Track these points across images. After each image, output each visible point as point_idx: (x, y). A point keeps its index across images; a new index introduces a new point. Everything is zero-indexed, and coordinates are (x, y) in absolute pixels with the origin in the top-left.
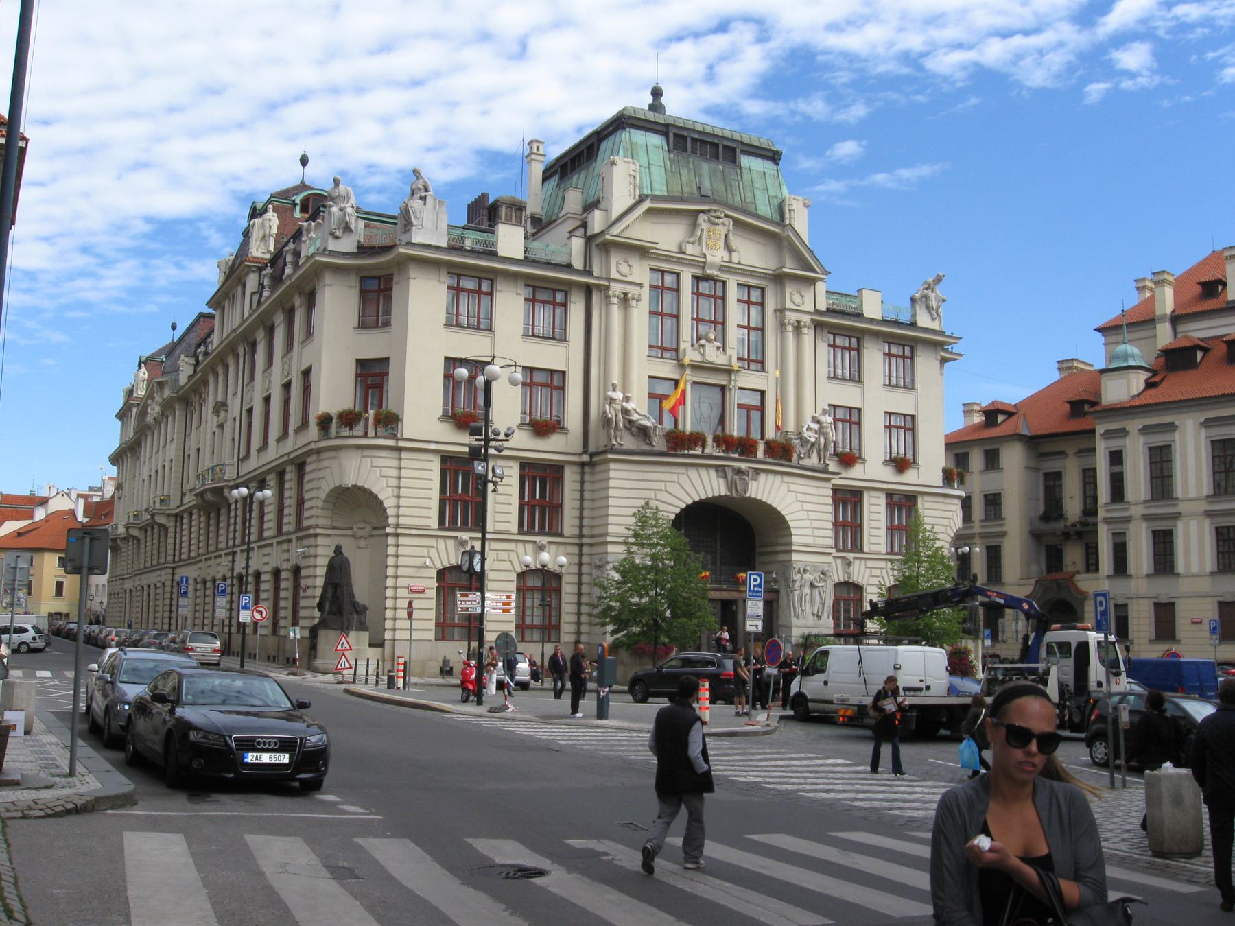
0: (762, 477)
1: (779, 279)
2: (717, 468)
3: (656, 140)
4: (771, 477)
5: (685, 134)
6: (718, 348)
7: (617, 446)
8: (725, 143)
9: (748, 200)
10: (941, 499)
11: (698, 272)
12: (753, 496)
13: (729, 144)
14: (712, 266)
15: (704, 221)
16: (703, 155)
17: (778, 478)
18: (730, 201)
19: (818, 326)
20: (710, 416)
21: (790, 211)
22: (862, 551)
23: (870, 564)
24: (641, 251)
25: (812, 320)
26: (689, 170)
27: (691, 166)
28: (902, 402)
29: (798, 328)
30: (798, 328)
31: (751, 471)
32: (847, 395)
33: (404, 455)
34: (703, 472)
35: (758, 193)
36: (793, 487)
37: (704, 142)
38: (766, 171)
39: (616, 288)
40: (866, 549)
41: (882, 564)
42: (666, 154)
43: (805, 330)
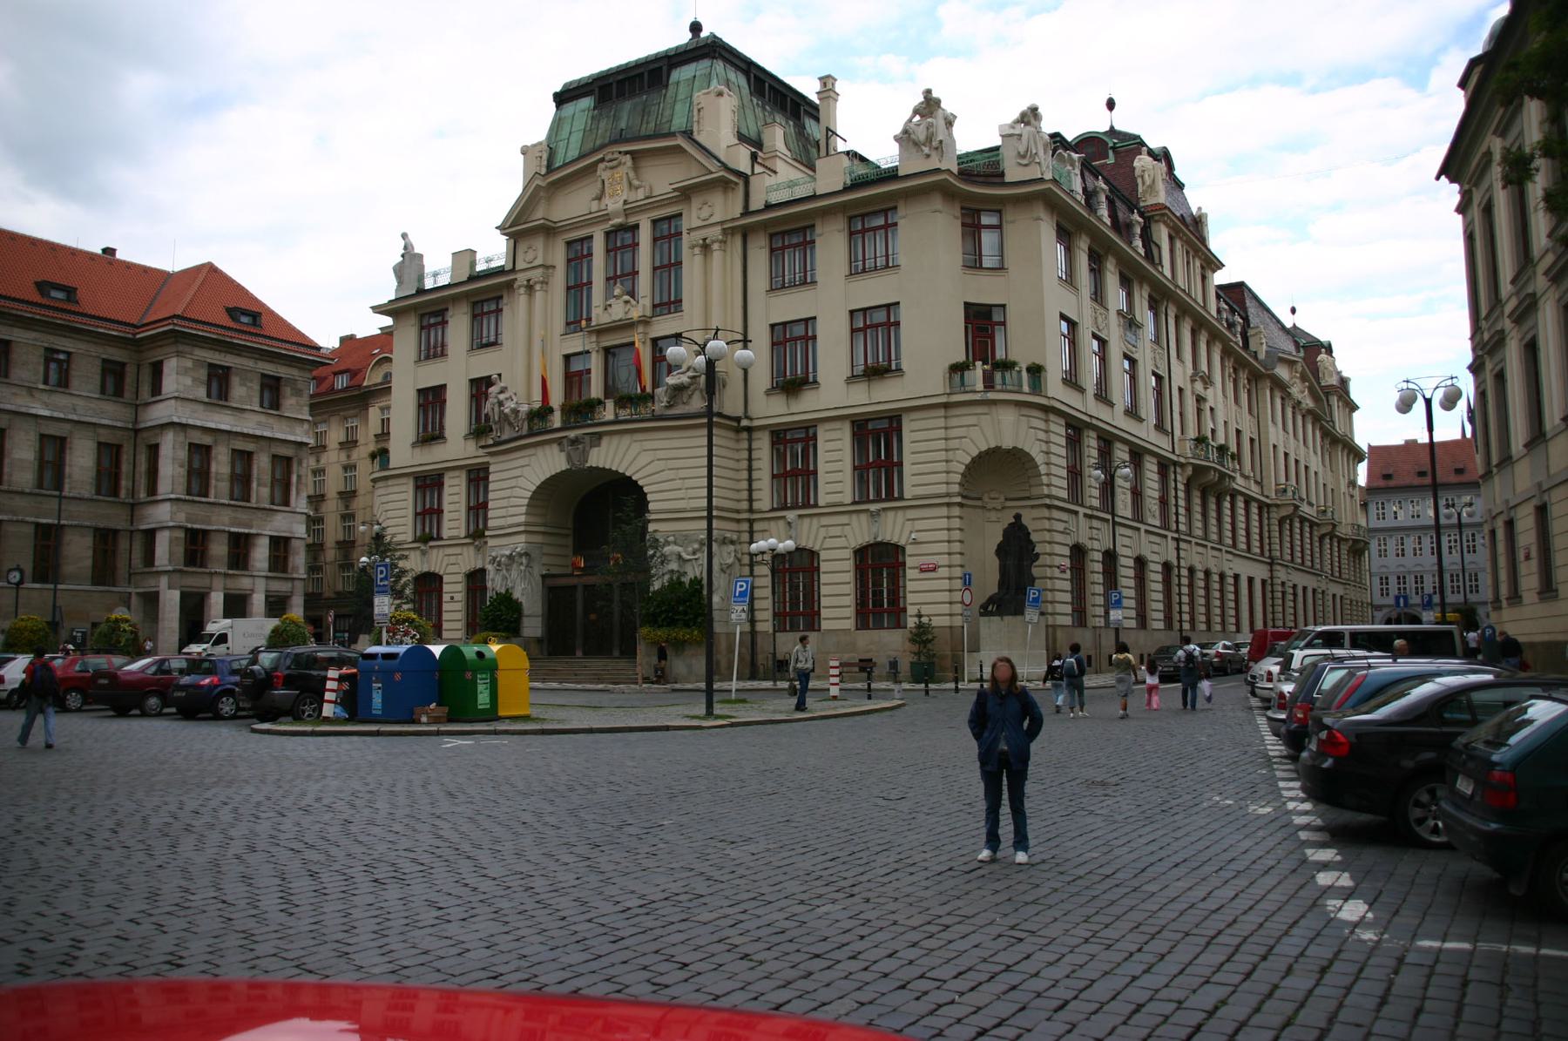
0: (605, 441)
1: (686, 194)
2: (559, 441)
3: (586, 103)
4: (615, 439)
5: (611, 80)
6: (627, 302)
7: (498, 439)
8: (652, 67)
9: (664, 120)
10: (942, 412)
11: (607, 226)
12: (594, 465)
13: (656, 65)
14: (616, 214)
15: (604, 170)
16: (633, 94)
17: (626, 439)
18: (643, 133)
19: (746, 233)
20: (627, 380)
21: (699, 110)
22: (816, 506)
23: (825, 521)
24: (548, 231)
25: (724, 229)
26: (608, 117)
27: (612, 113)
28: (873, 291)
29: (706, 247)
30: (706, 247)
31: (585, 436)
32: (790, 306)
33: (390, 482)
34: (547, 448)
35: (678, 107)
36: (648, 445)
37: (631, 79)
38: (698, 73)
39: (521, 278)
40: (821, 502)
41: (844, 519)
42: (590, 114)
43: (716, 246)
